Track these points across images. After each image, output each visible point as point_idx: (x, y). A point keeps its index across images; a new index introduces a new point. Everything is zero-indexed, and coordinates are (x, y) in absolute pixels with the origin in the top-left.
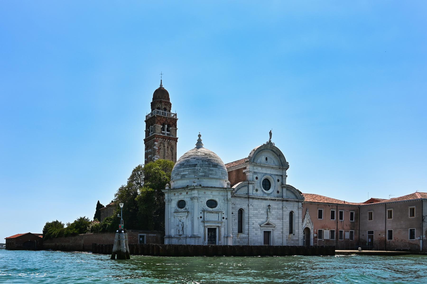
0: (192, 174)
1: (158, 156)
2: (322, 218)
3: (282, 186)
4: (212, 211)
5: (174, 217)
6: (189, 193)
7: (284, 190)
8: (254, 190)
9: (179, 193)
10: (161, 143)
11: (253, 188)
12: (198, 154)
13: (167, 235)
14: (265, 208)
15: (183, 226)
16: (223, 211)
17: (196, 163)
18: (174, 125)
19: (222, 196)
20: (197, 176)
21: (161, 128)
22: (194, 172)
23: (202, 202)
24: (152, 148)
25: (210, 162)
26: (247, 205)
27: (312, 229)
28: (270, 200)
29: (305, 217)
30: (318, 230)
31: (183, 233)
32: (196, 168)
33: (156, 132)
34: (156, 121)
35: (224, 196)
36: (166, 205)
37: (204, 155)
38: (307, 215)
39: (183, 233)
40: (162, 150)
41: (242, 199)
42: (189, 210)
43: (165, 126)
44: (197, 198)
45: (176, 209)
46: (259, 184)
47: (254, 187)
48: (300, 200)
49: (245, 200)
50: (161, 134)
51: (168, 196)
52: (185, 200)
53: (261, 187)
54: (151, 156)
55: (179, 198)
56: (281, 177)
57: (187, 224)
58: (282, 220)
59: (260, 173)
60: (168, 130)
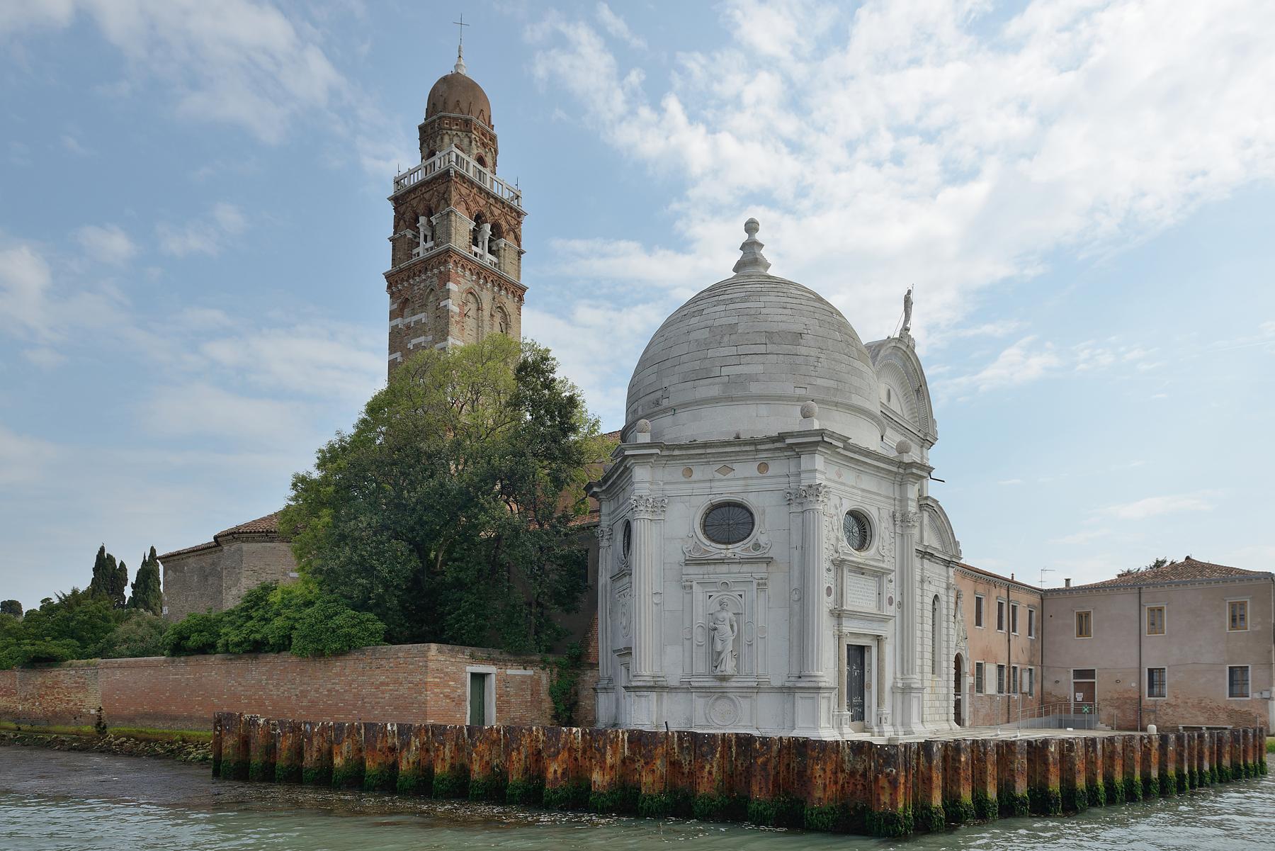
13: (648, 673)
15: (736, 628)
18: (514, 232)
24: (431, 308)
45: (697, 547)
52: (752, 501)
55: (715, 491)
60: (490, 251)
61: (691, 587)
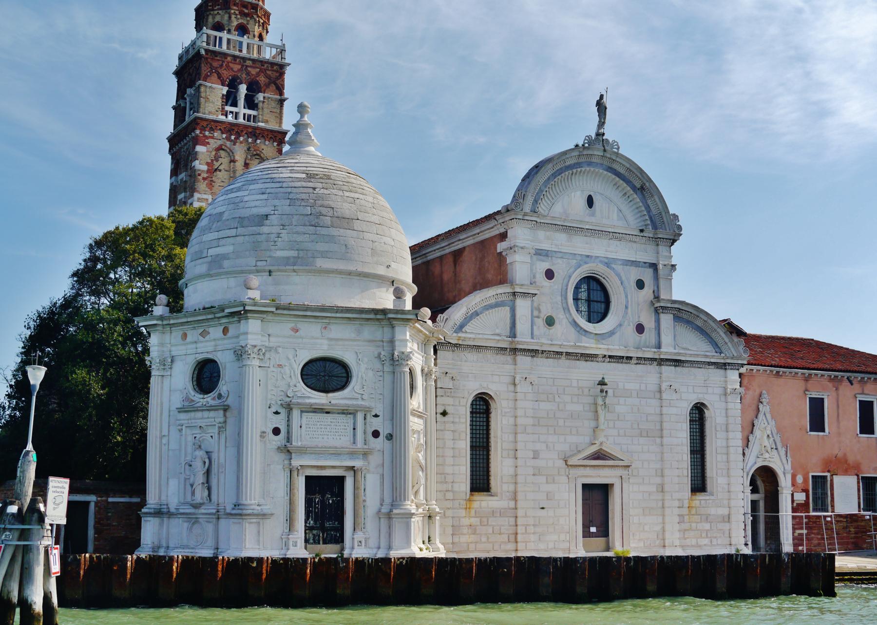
0: (247, 253)
1: (205, 196)
2: (823, 431)
3: (657, 305)
4: (323, 405)
5: (180, 427)
6: (231, 332)
7: (667, 320)
8: (540, 322)
9: (201, 330)
10: (220, 148)
11: (536, 313)
12: (281, 175)
14: (586, 391)
16: (373, 405)
17: (263, 211)
19: (370, 341)
20: (264, 263)
21: (223, 95)
22: (256, 247)
23: (280, 366)
25: (322, 206)
26: (508, 380)
27: (784, 473)
28: (608, 360)
29: (753, 425)
30: (811, 474)
31: (209, 495)
32: (265, 229)
33: (201, 110)
34: (205, 69)
35: (381, 343)
36: (152, 380)
37: (300, 180)
38: (761, 416)
39: (209, 495)
40: (221, 176)
41: (489, 354)
42: (229, 402)
43: (237, 90)
44: (256, 350)
45: (187, 399)
46: (559, 298)
47: (535, 310)
48: (729, 361)
49: (501, 358)
50: (223, 118)
51: (162, 344)
53: (566, 309)
54: (185, 197)
55: (199, 350)
56: (650, 271)
57: (222, 460)
58: (658, 440)
59: (563, 255)
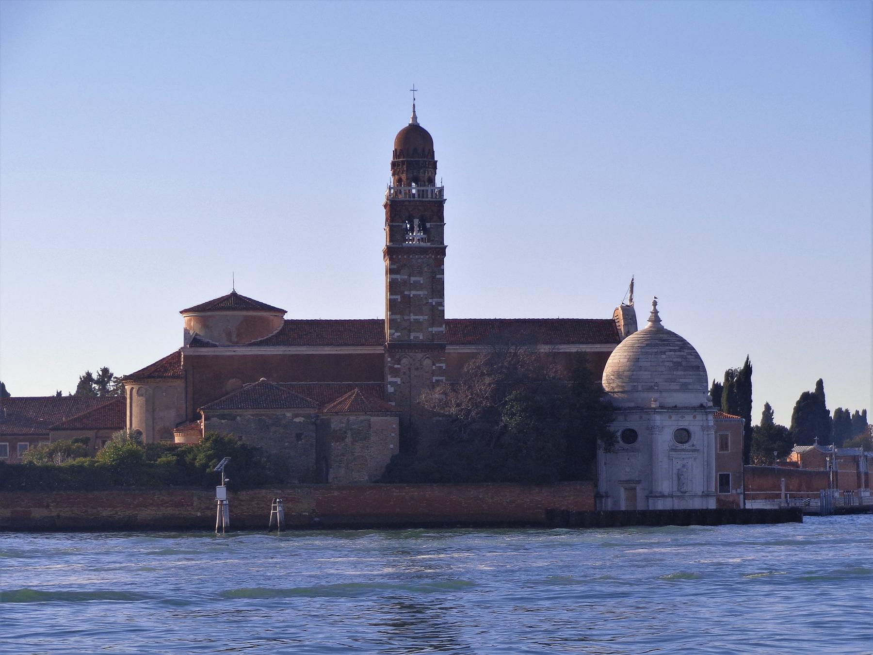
52: (692, 429)
55: (679, 424)
61: (672, 459)
